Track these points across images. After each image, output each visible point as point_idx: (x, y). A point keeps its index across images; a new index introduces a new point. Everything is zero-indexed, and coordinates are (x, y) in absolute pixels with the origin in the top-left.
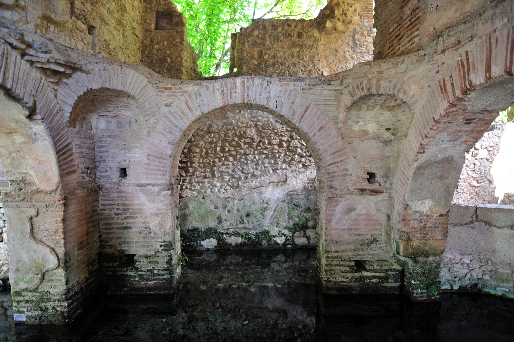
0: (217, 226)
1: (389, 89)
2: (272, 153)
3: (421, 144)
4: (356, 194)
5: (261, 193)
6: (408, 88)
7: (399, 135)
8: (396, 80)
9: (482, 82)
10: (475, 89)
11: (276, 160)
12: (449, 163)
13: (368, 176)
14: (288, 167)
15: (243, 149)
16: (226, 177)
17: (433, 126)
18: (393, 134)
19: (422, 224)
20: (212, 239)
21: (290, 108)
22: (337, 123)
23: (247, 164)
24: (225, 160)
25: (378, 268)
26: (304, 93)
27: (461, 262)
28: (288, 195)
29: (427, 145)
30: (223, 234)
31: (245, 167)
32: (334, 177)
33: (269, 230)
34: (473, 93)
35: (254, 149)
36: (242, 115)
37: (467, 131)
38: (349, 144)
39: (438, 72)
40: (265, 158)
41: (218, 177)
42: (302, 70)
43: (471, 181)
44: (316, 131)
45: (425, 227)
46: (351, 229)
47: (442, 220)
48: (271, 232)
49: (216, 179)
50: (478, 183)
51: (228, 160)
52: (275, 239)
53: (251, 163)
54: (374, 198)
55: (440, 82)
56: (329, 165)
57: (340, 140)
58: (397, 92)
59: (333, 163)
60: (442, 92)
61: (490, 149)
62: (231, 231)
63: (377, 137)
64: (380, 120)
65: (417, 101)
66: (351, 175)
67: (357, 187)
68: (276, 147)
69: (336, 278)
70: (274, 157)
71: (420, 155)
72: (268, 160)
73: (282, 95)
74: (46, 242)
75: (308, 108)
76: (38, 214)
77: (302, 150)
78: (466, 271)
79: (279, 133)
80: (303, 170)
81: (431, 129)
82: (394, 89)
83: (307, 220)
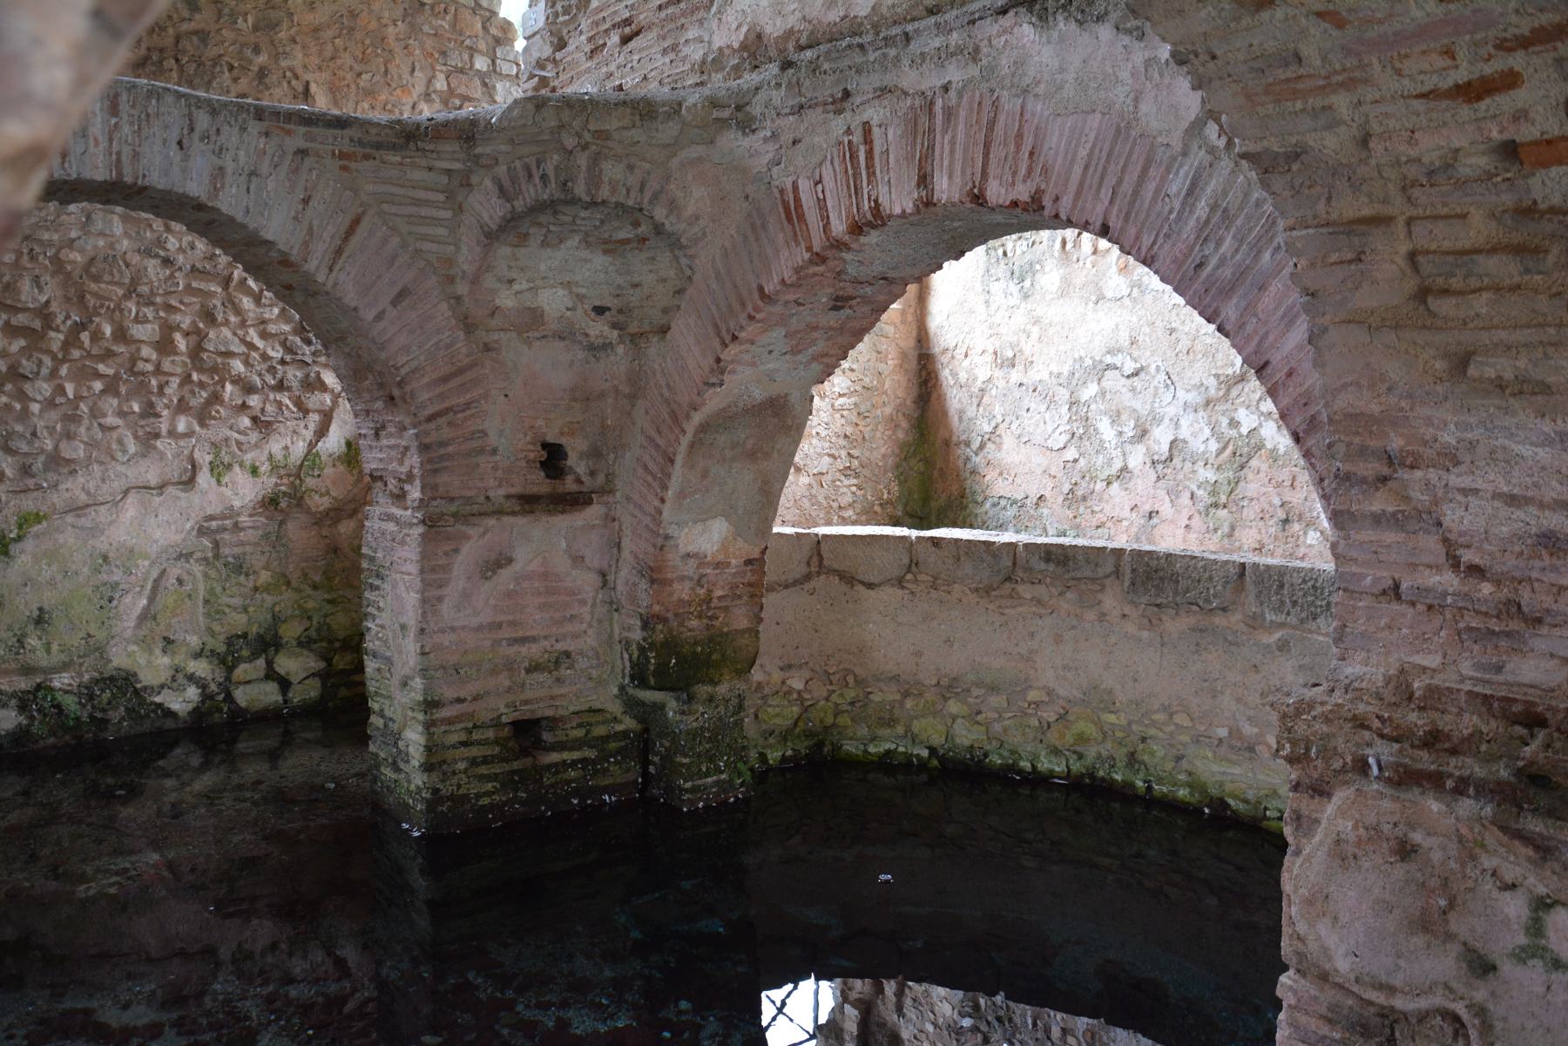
1: (628, 191)
2: (131, 371)
3: (718, 360)
4: (513, 513)
5: (96, 530)
6: (679, 194)
9: (909, 211)
10: (884, 224)
11: (151, 405)
12: (776, 415)
13: (544, 455)
14: (198, 428)
17: (757, 309)
18: (614, 326)
19: (702, 592)
21: (296, 218)
22: (451, 280)
23: (25, 414)
25: (579, 733)
26: (344, 168)
27: (785, 689)
28: (202, 532)
29: (733, 362)
31: (19, 428)
32: (441, 457)
34: (874, 233)
35: (54, 357)
37: (831, 328)
38: (488, 350)
40: (103, 392)
42: (231, 68)
45: (708, 600)
46: (500, 626)
48: (141, 676)
52: (158, 699)
53: (41, 411)
54: (563, 523)
55: (782, 192)
56: (430, 418)
57: (461, 335)
58: (651, 202)
60: (789, 219)
63: (566, 335)
64: (578, 278)
65: (704, 234)
66: (494, 451)
67: (512, 491)
68: (146, 352)
70: (141, 388)
72: (115, 402)
75: (356, 222)
77: (247, 363)
79: (158, 300)
80: (254, 437)
82: (641, 190)
83: (276, 618)
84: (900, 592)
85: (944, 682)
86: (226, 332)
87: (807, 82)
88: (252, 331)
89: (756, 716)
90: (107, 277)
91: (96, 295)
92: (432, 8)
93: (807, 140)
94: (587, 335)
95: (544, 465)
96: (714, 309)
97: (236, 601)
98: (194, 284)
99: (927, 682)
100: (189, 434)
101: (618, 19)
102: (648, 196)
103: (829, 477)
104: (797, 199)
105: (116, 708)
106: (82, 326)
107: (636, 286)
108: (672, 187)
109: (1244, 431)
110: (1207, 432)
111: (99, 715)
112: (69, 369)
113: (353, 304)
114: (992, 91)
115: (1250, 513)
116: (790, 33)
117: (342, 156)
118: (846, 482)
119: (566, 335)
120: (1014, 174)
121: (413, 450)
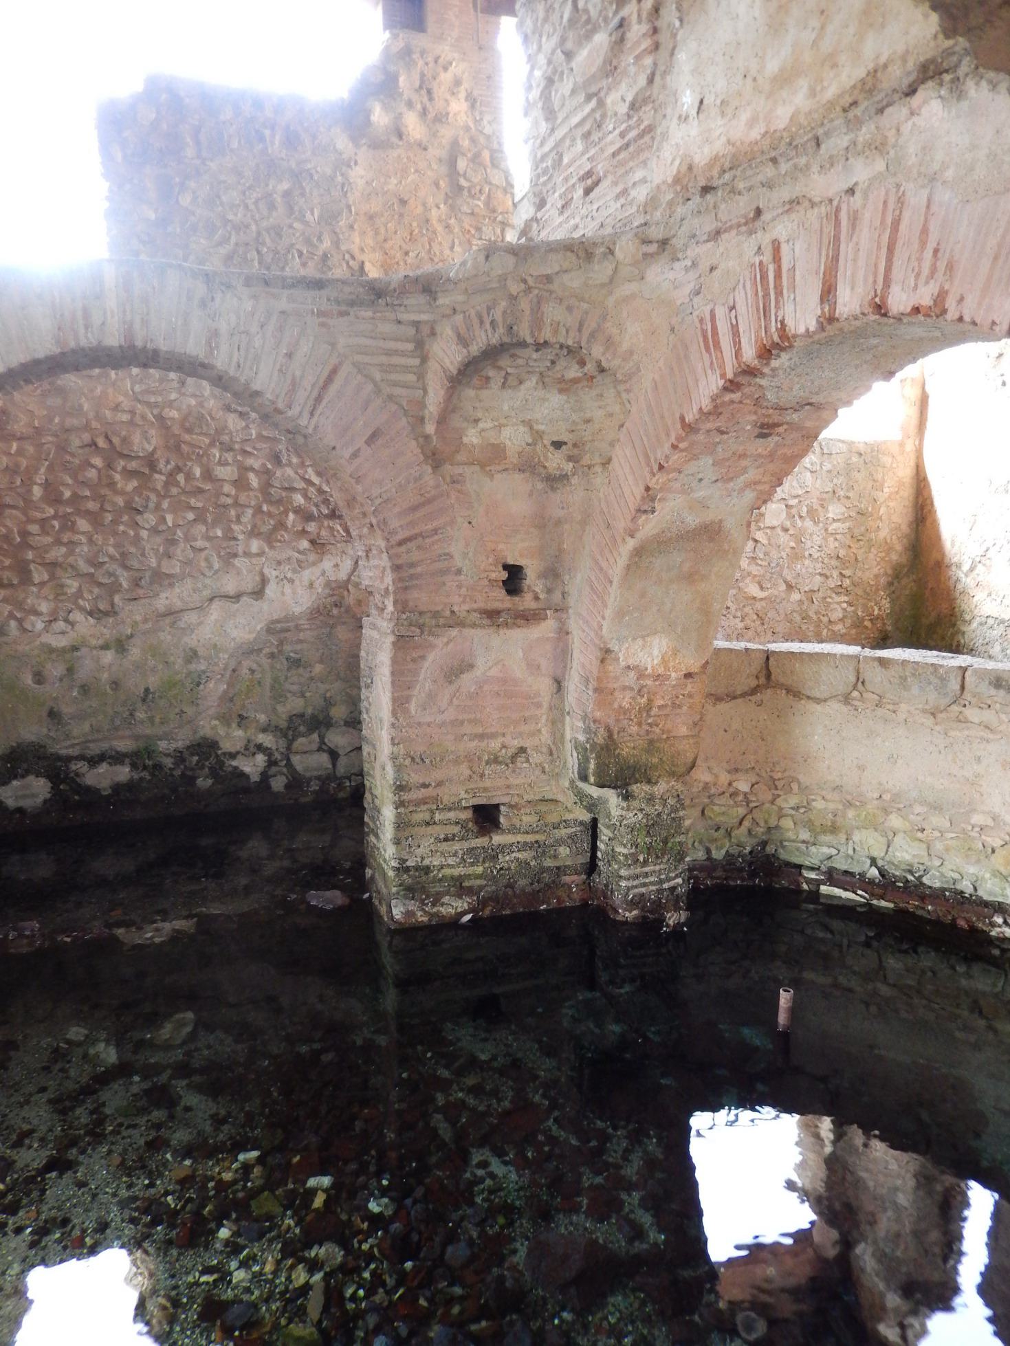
0: (47, 736)
1: (567, 332)
4: (474, 626)
5: (190, 629)
6: (615, 331)
7: (586, 460)
9: (812, 329)
10: (791, 346)
11: (230, 529)
12: (711, 540)
13: (505, 575)
15: (122, 493)
16: (69, 582)
18: (570, 458)
19: (644, 701)
20: (31, 778)
21: (280, 371)
23: (137, 538)
24: (64, 528)
26: (322, 325)
27: (732, 790)
28: (269, 630)
29: (661, 489)
30: (69, 759)
31: (133, 550)
32: (412, 577)
33: (217, 738)
34: (784, 356)
36: (114, 384)
37: (760, 456)
41: (42, 584)
42: (301, 254)
43: (747, 586)
44: (360, 442)
46: (462, 723)
47: (689, 686)
48: (221, 745)
49: (35, 589)
50: (762, 588)
51: (72, 528)
52: (234, 763)
55: (701, 320)
56: (400, 543)
57: (430, 470)
58: (588, 341)
59: (409, 539)
60: (707, 349)
61: (793, 502)
62: (94, 749)
64: (538, 416)
65: (638, 369)
66: (459, 572)
67: (475, 606)
68: (227, 488)
69: (423, 859)
71: (644, 517)
72: (204, 529)
73: (254, 328)
75: (334, 371)
77: (306, 496)
78: (741, 811)
79: (237, 446)
80: (312, 557)
81: (674, 447)
82: (580, 330)
83: (329, 703)
84: (844, 709)
86: (289, 471)
87: (723, 206)
88: (310, 470)
89: (703, 812)
90: (197, 430)
91: (189, 444)
92: (469, 191)
93: (722, 266)
94: (545, 467)
97: (295, 688)
98: (265, 433)
99: (870, 795)
100: (261, 554)
101: (582, 173)
102: (586, 334)
103: (821, 594)
105: (203, 767)
106: (178, 469)
107: (588, 421)
108: (609, 324)
111: (189, 773)
112: (170, 503)
113: (332, 444)
114: (898, 186)
116: (716, 158)
117: (321, 314)
118: (837, 599)
120: (918, 276)
121: (389, 570)
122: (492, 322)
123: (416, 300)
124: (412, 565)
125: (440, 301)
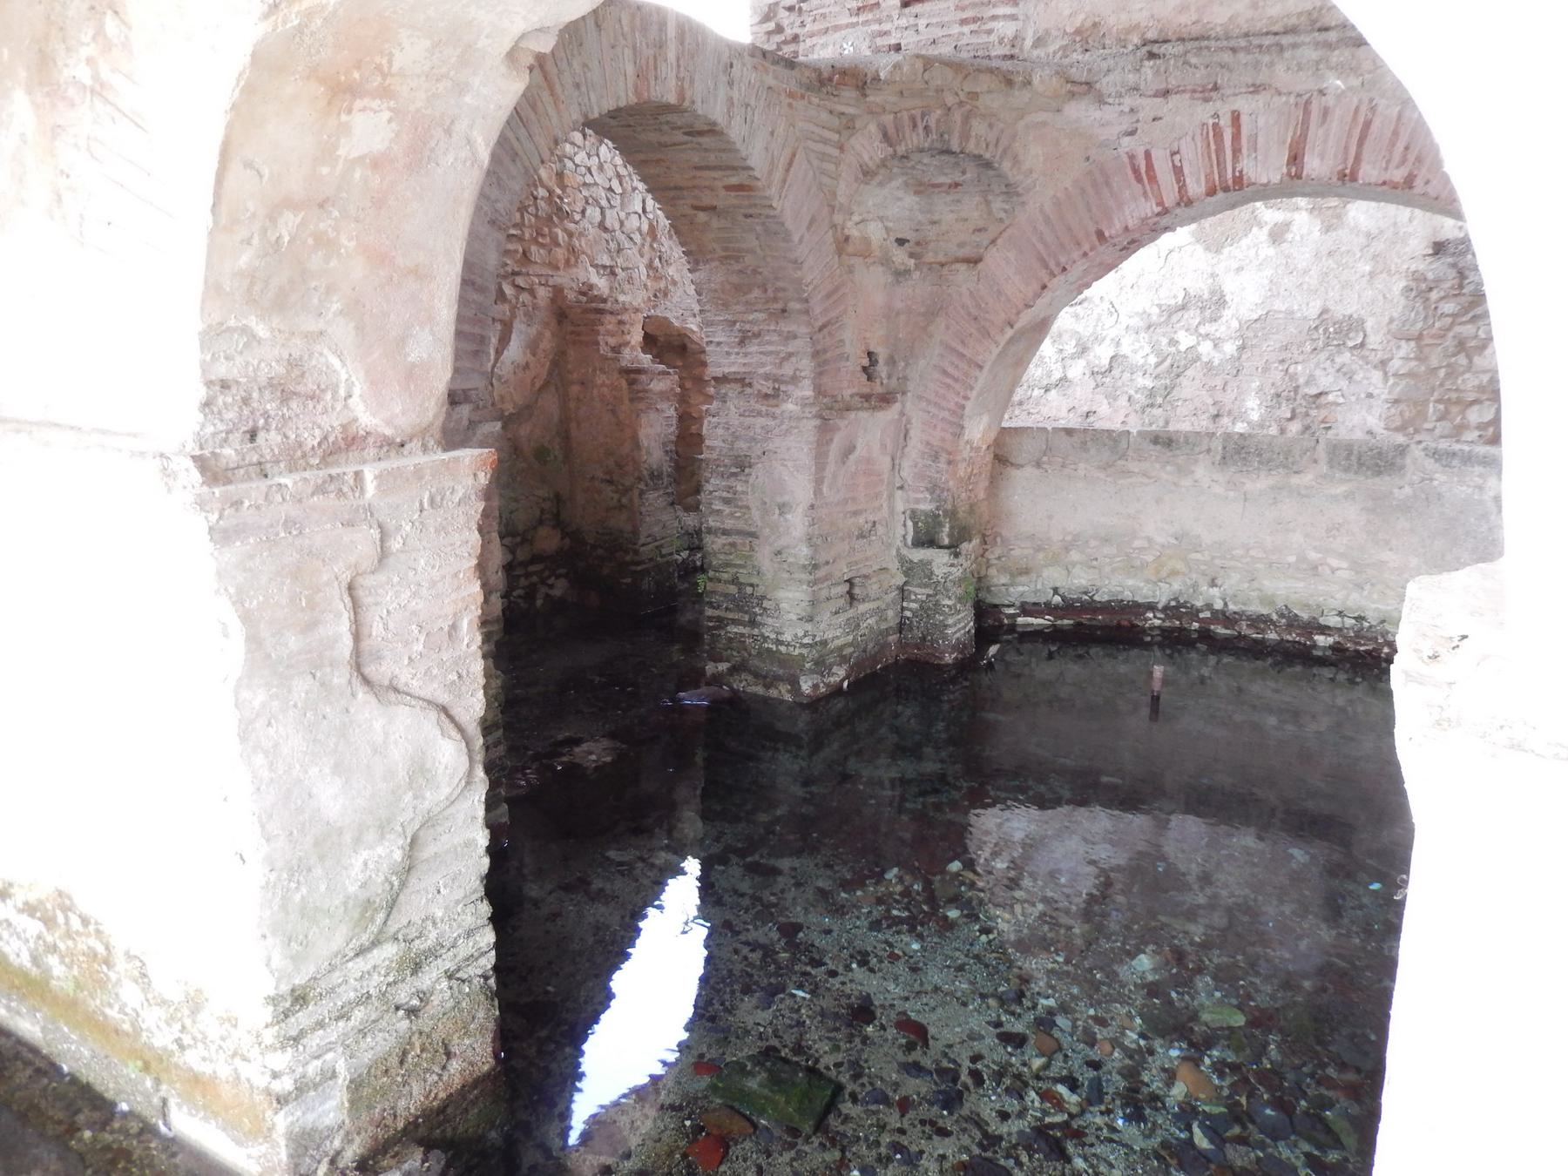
4: (858, 409)
8: (1001, 125)
18: (911, 255)
39: (1132, 133)
56: (820, 330)
60: (1139, 179)
74: (415, 685)
76: (384, 554)
84: (1037, 472)
85: (1069, 538)
95: (865, 369)
96: (1040, 247)
104: (1150, 166)
109: (1182, 348)
110: (1147, 349)
114: (1371, 100)
115: (1183, 410)
117: (791, 95)
119: (886, 261)
120: (1388, 162)
122: (926, 128)
123: (849, 94)
124: (825, 351)
125: (871, 99)
